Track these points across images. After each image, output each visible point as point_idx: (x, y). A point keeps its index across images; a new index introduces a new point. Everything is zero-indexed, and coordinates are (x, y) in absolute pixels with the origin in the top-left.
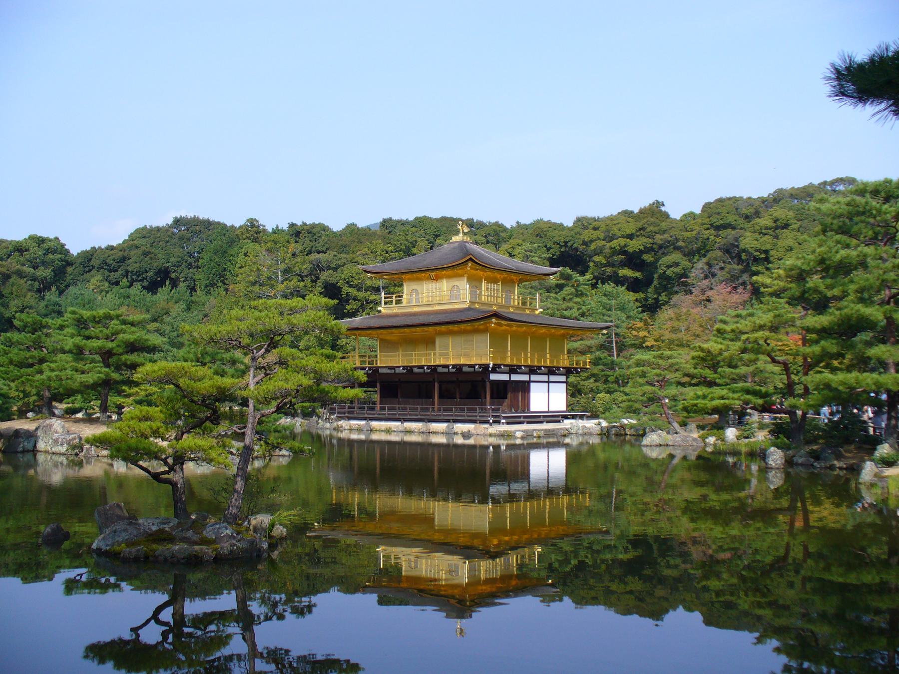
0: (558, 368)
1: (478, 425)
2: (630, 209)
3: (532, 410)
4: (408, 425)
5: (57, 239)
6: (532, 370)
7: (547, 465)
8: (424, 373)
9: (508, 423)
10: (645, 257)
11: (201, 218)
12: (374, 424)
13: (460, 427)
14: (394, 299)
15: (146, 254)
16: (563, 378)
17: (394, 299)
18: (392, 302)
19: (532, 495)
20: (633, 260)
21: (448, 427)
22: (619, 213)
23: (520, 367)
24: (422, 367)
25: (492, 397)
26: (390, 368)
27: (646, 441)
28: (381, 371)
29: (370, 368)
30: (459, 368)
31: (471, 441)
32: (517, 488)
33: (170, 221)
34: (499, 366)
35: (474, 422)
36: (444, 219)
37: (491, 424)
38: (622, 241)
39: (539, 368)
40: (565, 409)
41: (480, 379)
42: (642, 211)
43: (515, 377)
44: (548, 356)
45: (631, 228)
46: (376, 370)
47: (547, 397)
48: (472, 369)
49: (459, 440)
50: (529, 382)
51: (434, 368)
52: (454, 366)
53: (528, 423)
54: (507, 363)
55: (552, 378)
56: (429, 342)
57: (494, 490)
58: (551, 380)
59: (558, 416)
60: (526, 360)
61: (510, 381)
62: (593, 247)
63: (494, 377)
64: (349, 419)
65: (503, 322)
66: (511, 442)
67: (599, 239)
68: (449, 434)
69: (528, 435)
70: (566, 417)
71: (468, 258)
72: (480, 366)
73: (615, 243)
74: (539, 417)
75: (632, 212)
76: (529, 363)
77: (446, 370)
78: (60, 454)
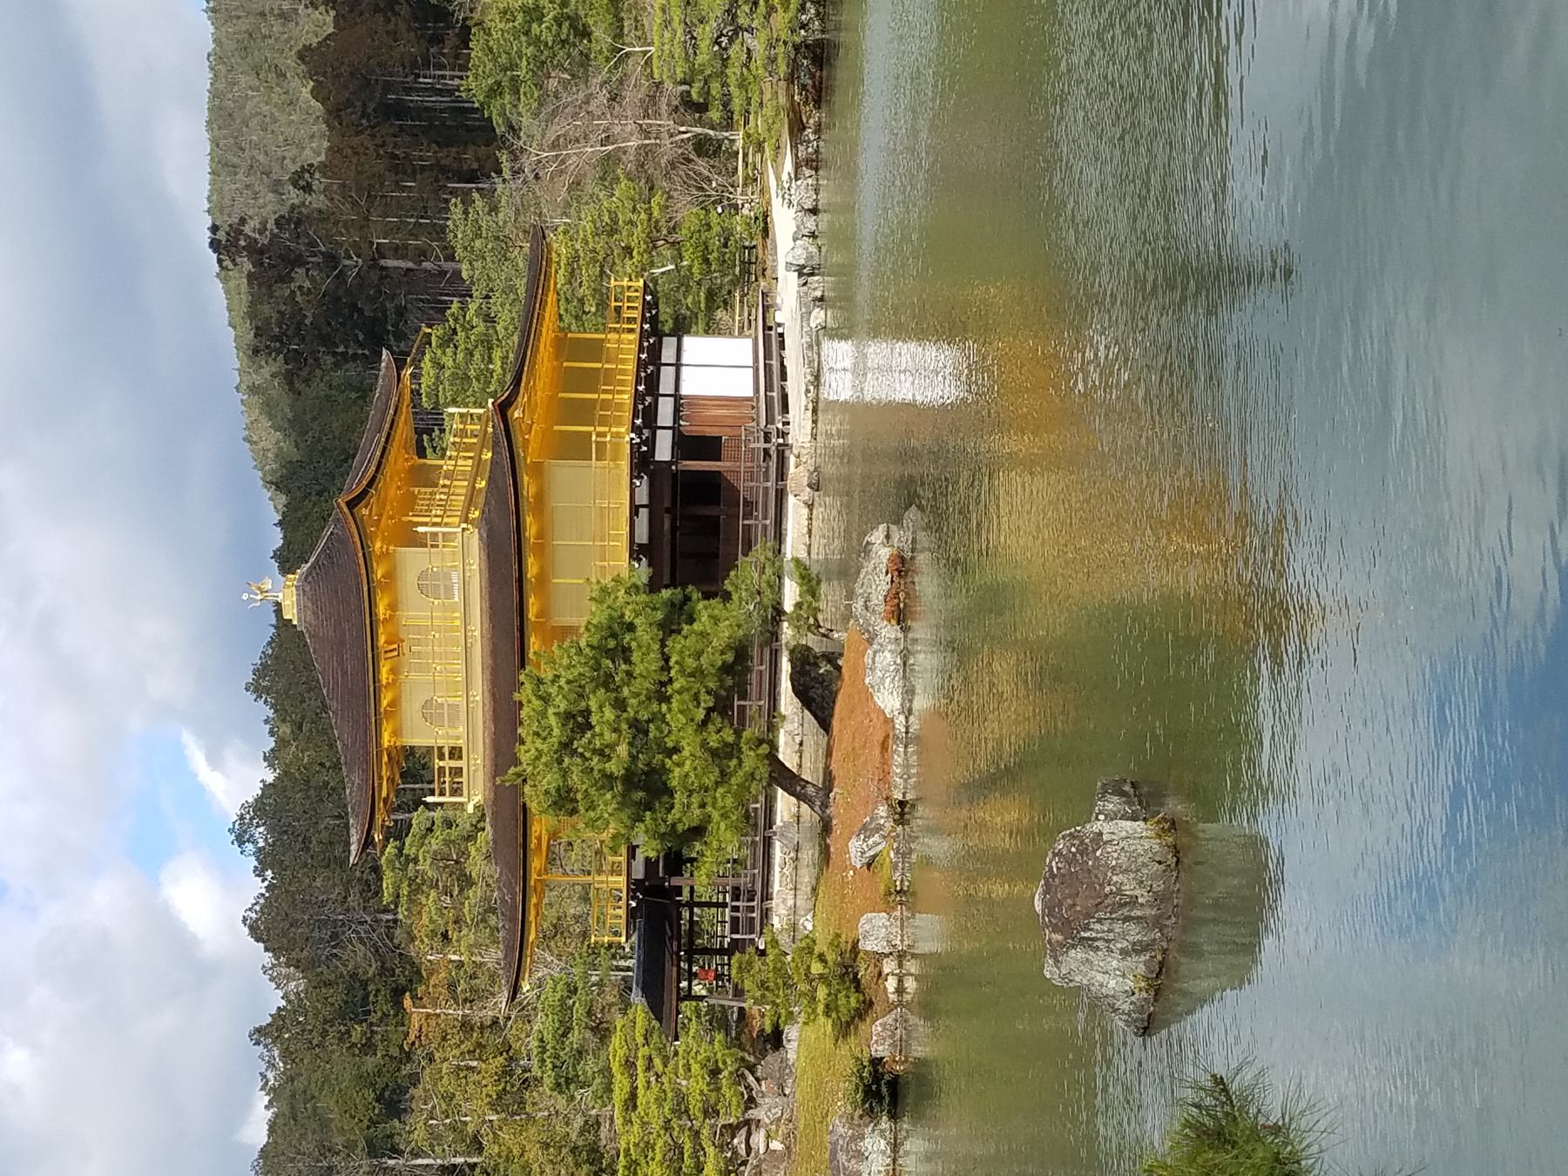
3: (750, 393)
14: (448, 763)
16: (669, 344)
17: (448, 763)
18: (459, 771)
25: (719, 460)
35: (781, 496)
40: (748, 343)
48: (644, 512)
50: (677, 396)
53: (784, 377)
55: (668, 355)
58: (673, 361)
63: (663, 452)
64: (767, 896)
65: (522, 399)
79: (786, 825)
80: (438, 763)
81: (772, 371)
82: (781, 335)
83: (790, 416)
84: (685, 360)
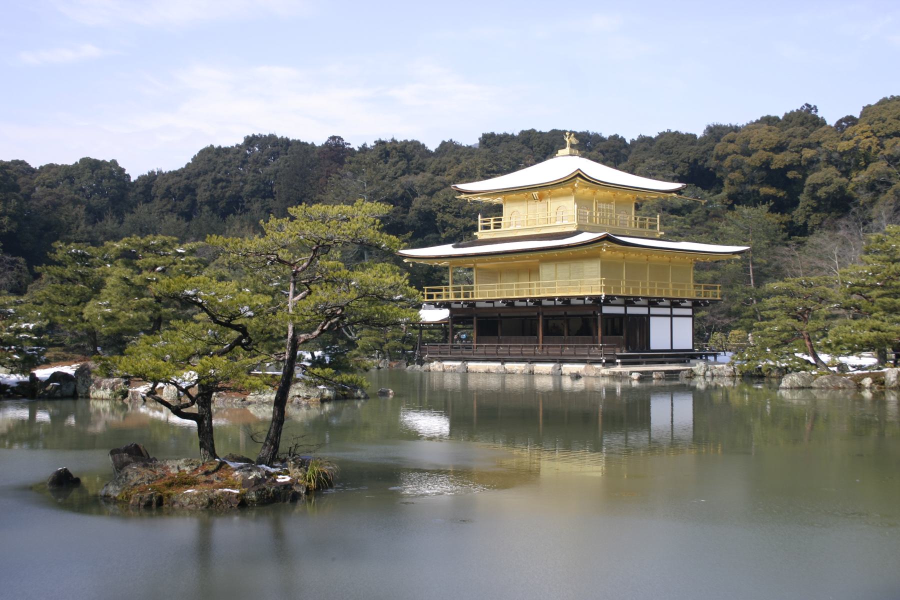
0: (683, 300)
1: (589, 367)
2: (773, 114)
3: (652, 347)
4: (509, 366)
5: (114, 163)
6: (653, 303)
7: (671, 413)
8: (527, 306)
9: (623, 364)
10: (791, 175)
11: (279, 136)
12: (472, 365)
13: (569, 368)
14: (492, 223)
15: (216, 181)
16: (689, 312)
19: (654, 447)
20: (775, 177)
21: (554, 368)
22: (757, 121)
23: (637, 299)
24: (524, 300)
25: (605, 333)
26: (488, 301)
27: (786, 382)
28: (478, 305)
29: (465, 302)
30: (566, 301)
31: (580, 384)
32: (637, 438)
33: (241, 141)
34: (612, 298)
36: (555, 132)
37: (604, 365)
39: (660, 299)
41: (592, 312)
42: (789, 117)
43: (631, 310)
44: (671, 286)
45: (775, 137)
46: (472, 304)
47: (670, 332)
48: (581, 302)
49: (567, 383)
50: (649, 316)
51: (538, 302)
52: (560, 298)
54: (622, 294)
55: (676, 311)
56: (532, 272)
59: (684, 356)
60: (644, 290)
61: (626, 315)
62: (727, 162)
63: (606, 310)
64: (441, 360)
66: (627, 383)
67: (735, 152)
68: (558, 375)
69: (645, 377)
70: (693, 357)
72: (591, 298)
74: (661, 356)
75: (776, 119)
76: (648, 294)
77: (552, 303)
78: (102, 399)
80: (492, 219)
82: (684, 362)
84: (674, 319)
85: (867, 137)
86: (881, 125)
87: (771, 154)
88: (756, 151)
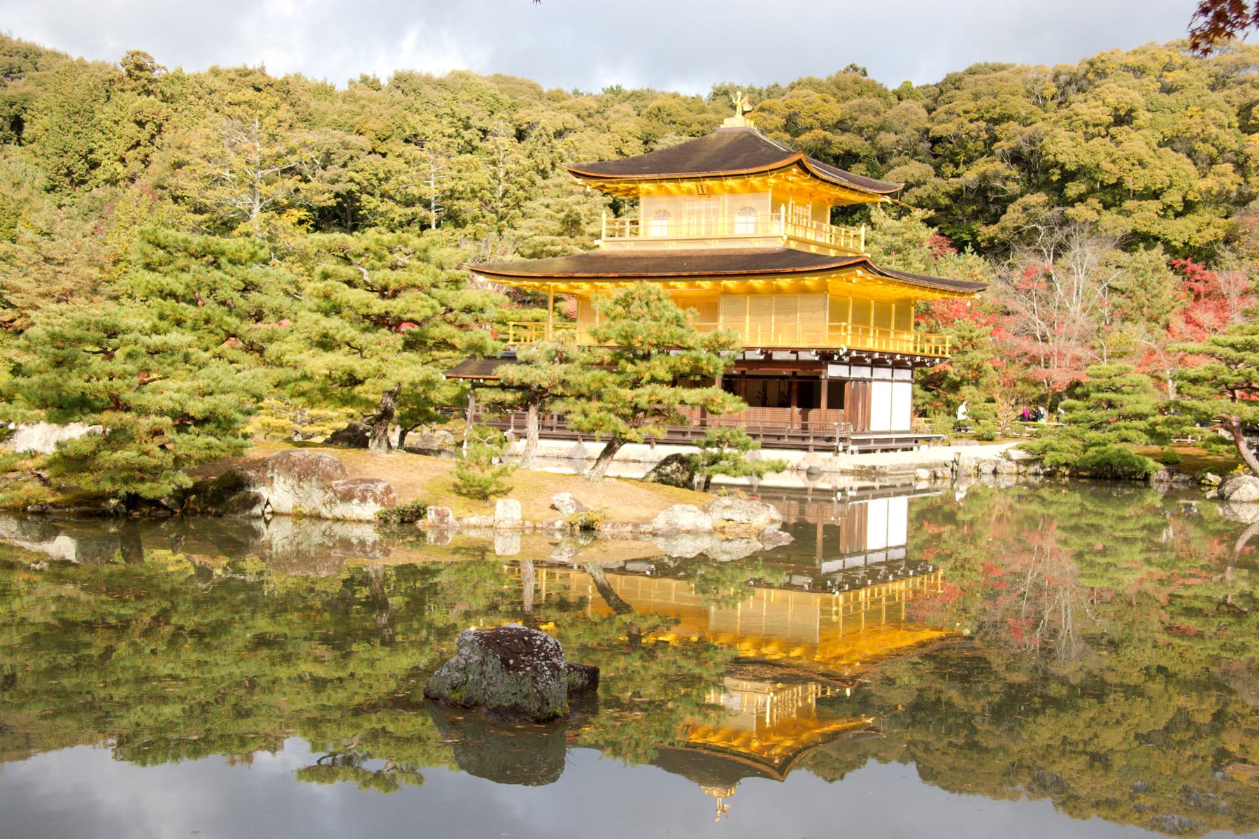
3: (873, 428)
9: (861, 452)
16: (906, 374)
19: (873, 574)
25: (830, 406)
32: (858, 561)
35: (805, 449)
38: (820, 133)
45: (835, 110)
48: (793, 357)
50: (870, 381)
57: (827, 567)
63: (834, 371)
71: (796, 158)
73: (806, 137)
74: (889, 440)
75: (820, 84)
79: (585, 451)
81: (887, 445)
83: (857, 455)
84: (895, 384)
85: (971, 121)
86: (992, 101)
87: (829, 135)
88: (811, 128)
